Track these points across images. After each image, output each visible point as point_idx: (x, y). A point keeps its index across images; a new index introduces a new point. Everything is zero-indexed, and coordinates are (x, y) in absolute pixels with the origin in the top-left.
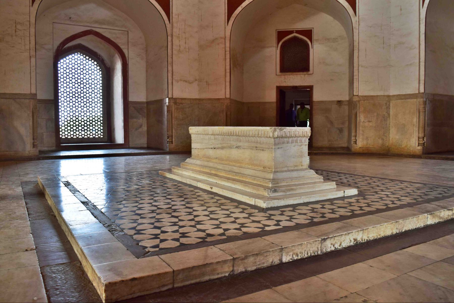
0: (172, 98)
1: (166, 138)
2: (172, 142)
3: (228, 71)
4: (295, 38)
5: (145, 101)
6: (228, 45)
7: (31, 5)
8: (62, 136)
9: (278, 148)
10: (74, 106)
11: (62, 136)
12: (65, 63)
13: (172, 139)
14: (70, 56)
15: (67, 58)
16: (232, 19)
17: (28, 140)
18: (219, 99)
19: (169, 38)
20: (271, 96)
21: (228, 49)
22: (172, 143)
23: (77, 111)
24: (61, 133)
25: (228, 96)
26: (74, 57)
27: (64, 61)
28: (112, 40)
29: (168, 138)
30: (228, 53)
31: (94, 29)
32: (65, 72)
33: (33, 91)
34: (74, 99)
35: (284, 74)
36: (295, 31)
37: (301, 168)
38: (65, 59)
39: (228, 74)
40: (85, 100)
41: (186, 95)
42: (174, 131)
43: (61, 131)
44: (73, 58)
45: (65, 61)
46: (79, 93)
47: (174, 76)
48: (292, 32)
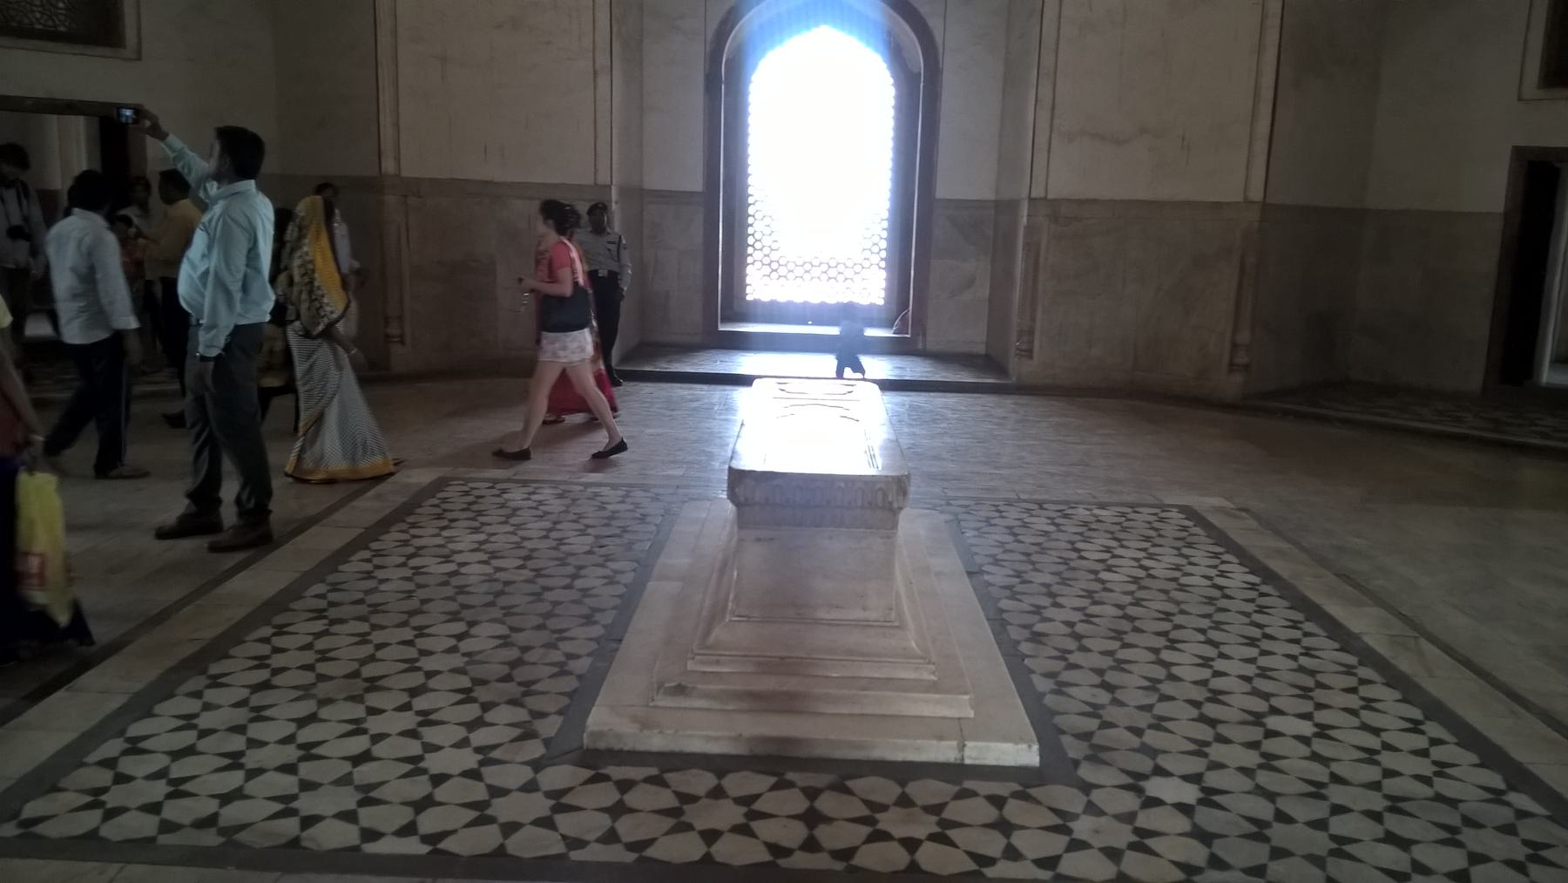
0: (1045, 198)
1: (1014, 336)
2: (1029, 353)
3: (1267, 94)
5: (990, 196)
9: (758, 540)
13: (1031, 342)
18: (1218, 206)
22: (1031, 358)
29: (1021, 333)
30: (1274, 22)
33: (603, 178)
37: (858, 614)
42: (1039, 315)
47: (1056, 122)
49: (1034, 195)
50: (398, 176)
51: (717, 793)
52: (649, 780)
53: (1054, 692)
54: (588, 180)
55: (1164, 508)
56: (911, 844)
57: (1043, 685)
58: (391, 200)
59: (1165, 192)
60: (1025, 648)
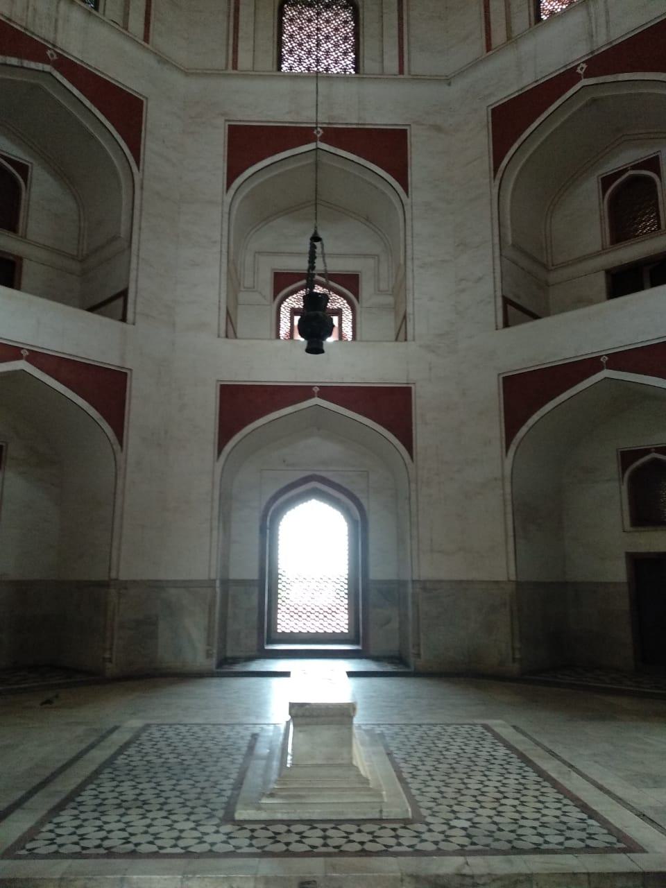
2: (418, 655)
3: (511, 533)
4: (655, 461)
6: (508, 490)
7: (216, 458)
13: (419, 650)
16: (513, 448)
17: (201, 647)
18: (497, 582)
19: (413, 486)
20: (618, 572)
21: (509, 497)
25: (513, 578)
28: (344, 485)
30: (509, 503)
31: (318, 473)
33: (213, 576)
35: (640, 529)
36: (653, 450)
39: (511, 540)
41: (443, 575)
48: (646, 451)
49: (414, 579)
50: (117, 580)
51: (289, 831)
52: (262, 829)
53: (419, 795)
54: (205, 577)
55: (475, 725)
56: (362, 843)
57: (414, 792)
58: (113, 591)
59: (474, 575)
60: (418, 798)
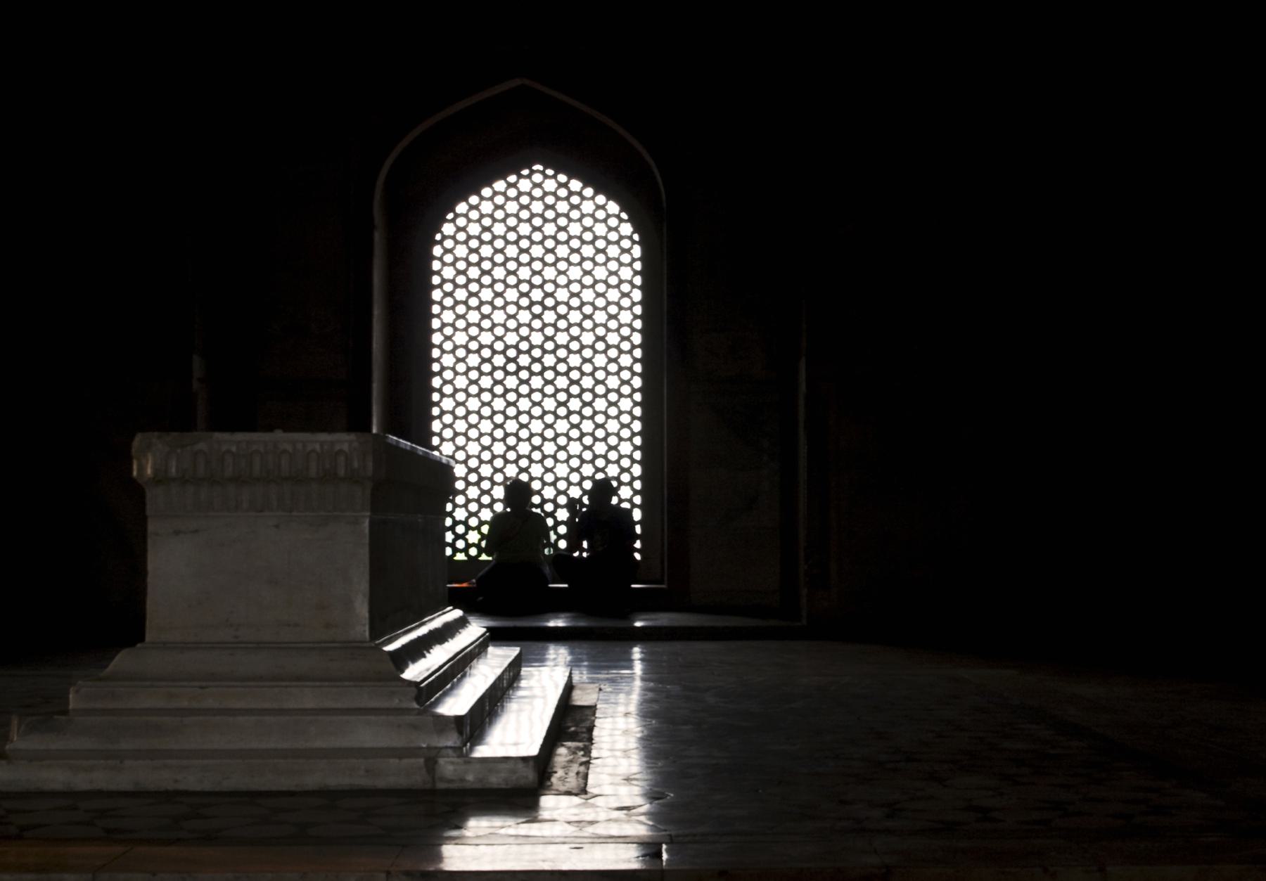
8: (455, 550)
10: (511, 411)
11: (455, 550)
12: (474, 215)
14: (500, 185)
15: (486, 192)
23: (524, 434)
24: (449, 537)
26: (514, 185)
27: (472, 207)
32: (474, 258)
34: (511, 382)
38: (474, 200)
40: (562, 382)
43: (452, 528)
44: (512, 193)
45: (476, 207)
46: (537, 353)
